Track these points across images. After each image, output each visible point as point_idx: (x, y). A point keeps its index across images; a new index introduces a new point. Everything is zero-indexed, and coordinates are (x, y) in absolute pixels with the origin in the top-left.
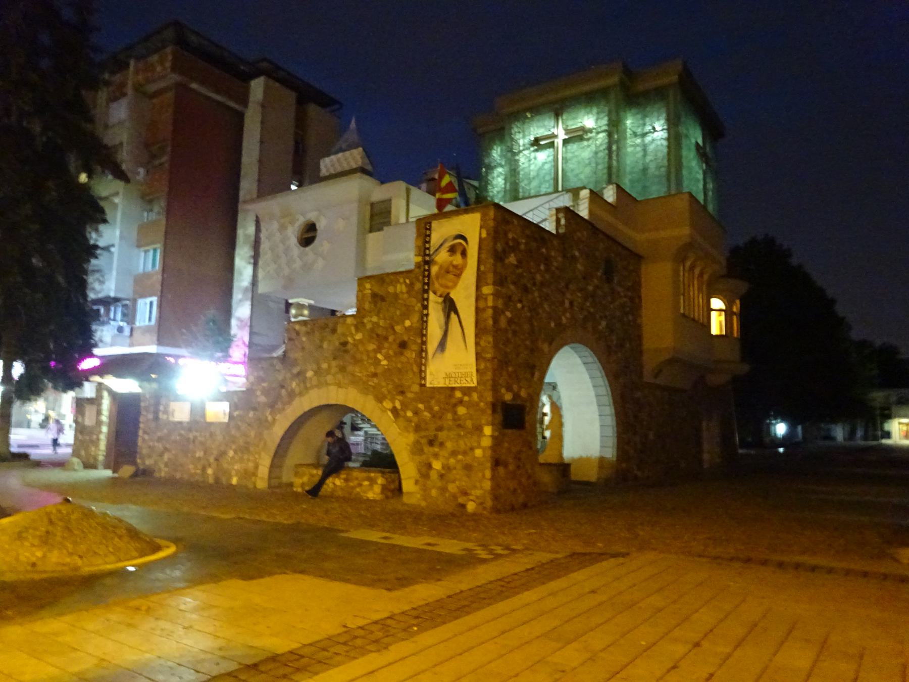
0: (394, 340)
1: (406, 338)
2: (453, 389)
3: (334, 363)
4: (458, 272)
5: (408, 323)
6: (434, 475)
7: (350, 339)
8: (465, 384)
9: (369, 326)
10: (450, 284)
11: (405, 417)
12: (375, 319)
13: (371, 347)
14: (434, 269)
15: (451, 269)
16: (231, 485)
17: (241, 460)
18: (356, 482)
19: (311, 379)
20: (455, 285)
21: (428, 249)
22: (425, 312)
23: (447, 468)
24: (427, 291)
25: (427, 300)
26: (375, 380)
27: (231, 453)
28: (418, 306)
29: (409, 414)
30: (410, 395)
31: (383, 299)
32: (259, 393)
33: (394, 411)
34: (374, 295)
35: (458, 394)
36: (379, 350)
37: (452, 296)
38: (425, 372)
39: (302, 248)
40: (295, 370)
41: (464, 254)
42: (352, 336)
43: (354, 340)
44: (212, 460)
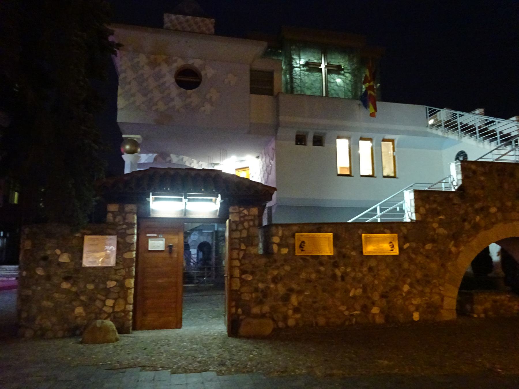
16: (413, 321)
17: (422, 294)
19: (494, 214)
27: (406, 288)
32: (435, 225)
39: (183, 90)
40: (477, 206)
44: (376, 297)
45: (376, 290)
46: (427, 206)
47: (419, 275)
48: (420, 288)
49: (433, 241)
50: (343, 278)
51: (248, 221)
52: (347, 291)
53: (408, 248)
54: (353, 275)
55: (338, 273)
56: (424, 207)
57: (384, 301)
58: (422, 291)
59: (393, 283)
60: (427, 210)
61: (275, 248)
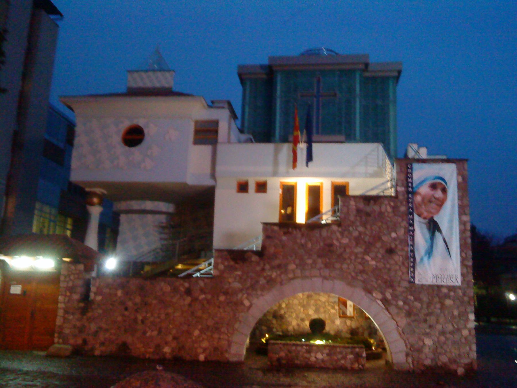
0: (382, 247)
1: (393, 246)
2: (439, 287)
3: (319, 261)
4: (440, 203)
5: (394, 235)
6: (426, 350)
7: (335, 242)
8: (450, 283)
9: (356, 234)
10: (433, 211)
11: (397, 306)
12: (361, 229)
13: (359, 250)
14: (418, 198)
15: (433, 199)
16: (198, 361)
18: (340, 356)
20: (438, 211)
21: (412, 183)
22: (411, 228)
23: (438, 345)
24: (412, 214)
25: (413, 220)
26: (365, 276)
27: (196, 333)
28: (404, 224)
29: (401, 303)
30: (399, 289)
31: (368, 214)
33: (385, 301)
34: (359, 211)
35: (445, 291)
36: (367, 252)
37: (436, 218)
38: (414, 272)
41: (444, 191)
42: (337, 240)
43: (340, 243)
44: (170, 338)
45: (170, 333)
46: (226, 263)
47: (210, 322)
48: (209, 333)
49: (226, 293)
50: (143, 321)
51: (74, 274)
52: (145, 333)
53: (203, 299)
54: (152, 319)
55: (140, 318)
56: (223, 263)
57: (175, 341)
58: (212, 336)
59: (185, 328)
60: (225, 267)
61: (92, 295)
